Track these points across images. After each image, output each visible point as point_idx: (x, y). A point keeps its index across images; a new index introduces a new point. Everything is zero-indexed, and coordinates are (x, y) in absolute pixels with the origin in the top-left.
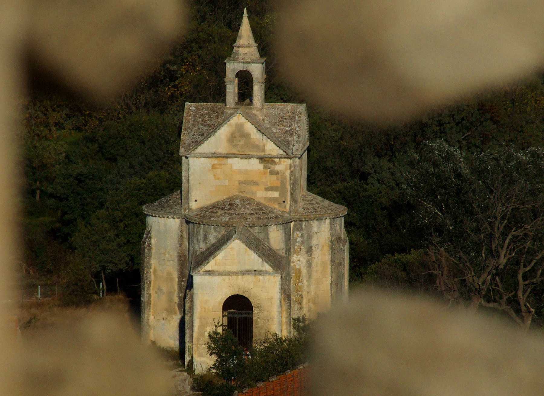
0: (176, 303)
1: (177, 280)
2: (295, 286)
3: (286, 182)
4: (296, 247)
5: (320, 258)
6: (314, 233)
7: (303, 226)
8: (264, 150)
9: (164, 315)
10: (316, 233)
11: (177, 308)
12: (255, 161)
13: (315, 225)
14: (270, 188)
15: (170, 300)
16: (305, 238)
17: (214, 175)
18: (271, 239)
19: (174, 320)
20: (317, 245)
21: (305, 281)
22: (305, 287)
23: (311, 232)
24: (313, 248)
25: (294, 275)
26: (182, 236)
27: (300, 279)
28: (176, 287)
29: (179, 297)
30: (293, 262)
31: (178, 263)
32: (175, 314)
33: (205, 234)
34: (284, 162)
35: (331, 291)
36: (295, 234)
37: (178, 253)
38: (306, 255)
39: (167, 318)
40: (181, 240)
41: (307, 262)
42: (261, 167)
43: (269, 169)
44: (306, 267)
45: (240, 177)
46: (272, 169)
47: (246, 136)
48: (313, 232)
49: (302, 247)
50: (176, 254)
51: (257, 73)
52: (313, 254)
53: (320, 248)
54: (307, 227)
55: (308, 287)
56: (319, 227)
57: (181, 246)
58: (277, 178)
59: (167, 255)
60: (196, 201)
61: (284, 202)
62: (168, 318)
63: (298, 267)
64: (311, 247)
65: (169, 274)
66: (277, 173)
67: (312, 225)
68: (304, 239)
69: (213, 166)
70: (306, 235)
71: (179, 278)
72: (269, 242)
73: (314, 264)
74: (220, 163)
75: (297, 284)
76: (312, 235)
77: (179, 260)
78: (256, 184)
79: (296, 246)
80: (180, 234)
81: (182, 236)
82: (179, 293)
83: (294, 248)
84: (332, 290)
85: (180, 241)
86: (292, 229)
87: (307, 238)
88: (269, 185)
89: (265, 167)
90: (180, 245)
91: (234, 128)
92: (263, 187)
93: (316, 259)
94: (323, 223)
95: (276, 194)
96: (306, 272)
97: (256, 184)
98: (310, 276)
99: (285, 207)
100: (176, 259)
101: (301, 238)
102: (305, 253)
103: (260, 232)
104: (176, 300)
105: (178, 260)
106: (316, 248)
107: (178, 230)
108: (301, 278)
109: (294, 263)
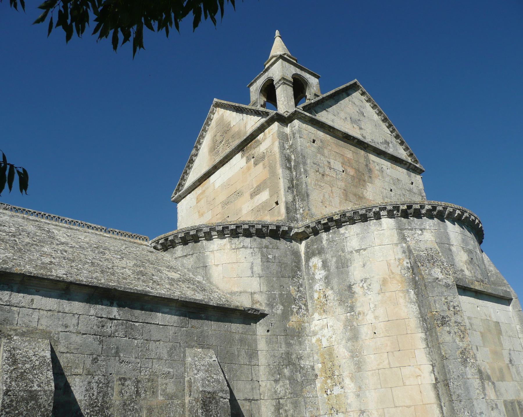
2: (325, 396)
3: (276, 162)
4: (316, 296)
5: (380, 311)
6: (352, 252)
7: (324, 242)
10: (358, 251)
13: (352, 233)
14: (256, 190)
16: (333, 268)
18: (214, 268)
20: (364, 280)
21: (347, 382)
22: (351, 399)
23: (343, 251)
24: (356, 288)
25: (320, 366)
27: (333, 374)
30: (315, 334)
34: (269, 133)
35: (441, 408)
36: (311, 264)
38: (340, 310)
41: (345, 327)
43: (253, 157)
44: (344, 342)
48: (350, 250)
49: (329, 292)
51: (278, 73)
52: (358, 304)
53: (376, 287)
54: (333, 241)
55: (358, 396)
56: (363, 239)
61: (277, 203)
63: (325, 343)
64: (350, 287)
66: (263, 157)
67: (343, 234)
68: (329, 270)
70: (334, 260)
72: (207, 276)
73: (365, 331)
74: (204, 189)
75: (329, 393)
76: (348, 256)
79: (316, 291)
83: (312, 297)
84: (443, 404)
86: (303, 256)
87: (337, 268)
91: (215, 130)
92: (247, 195)
93: (370, 318)
94: (373, 228)
95: (264, 196)
96: (347, 354)
97: (239, 194)
98: (359, 366)
99: (279, 212)
101: (323, 271)
102: (337, 303)
103: (186, 256)
106: (363, 287)
108: (337, 373)
109: (318, 336)
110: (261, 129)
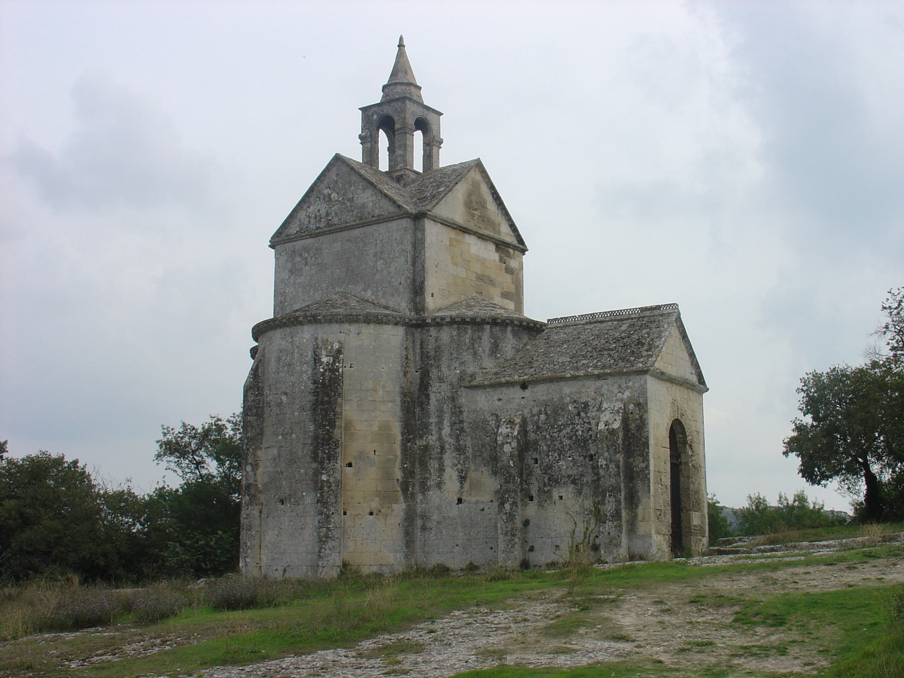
0: (398, 480)
1: (399, 438)
8: (499, 232)
9: (375, 505)
11: (399, 489)
12: (492, 247)
15: (387, 475)
17: (452, 257)
19: (394, 513)
26: (407, 358)
28: (399, 453)
29: (404, 470)
31: (402, 406)
32: (396, 501)
33: (495, 342)
37: (402, 387)
39: (380, 511)
40: (406, 364)
42: (495, 256)
43: (504, 263)
45: (477, 268)
46: (507, 263)
47: (482, 205)
50: (397, 389)
57: (405, 374)
58: (512, 279)
59: (381, 393)
60: (432, 294)
62: (383, 511)
65: (385, 427)
69: (450, 241)
71: (403, 434)
77: (403, 402)
78: (492, 282)
80: (404, 353)
81: (407, 358)
82: (403, 463)
85: (405, 368)
88: (505, 289)
89: (501, 260)
90: (405, 373)
100: (398, 399)
104: (398, 474)
105: (401, 401)
107: (402, 345)
110: (515, 248)
